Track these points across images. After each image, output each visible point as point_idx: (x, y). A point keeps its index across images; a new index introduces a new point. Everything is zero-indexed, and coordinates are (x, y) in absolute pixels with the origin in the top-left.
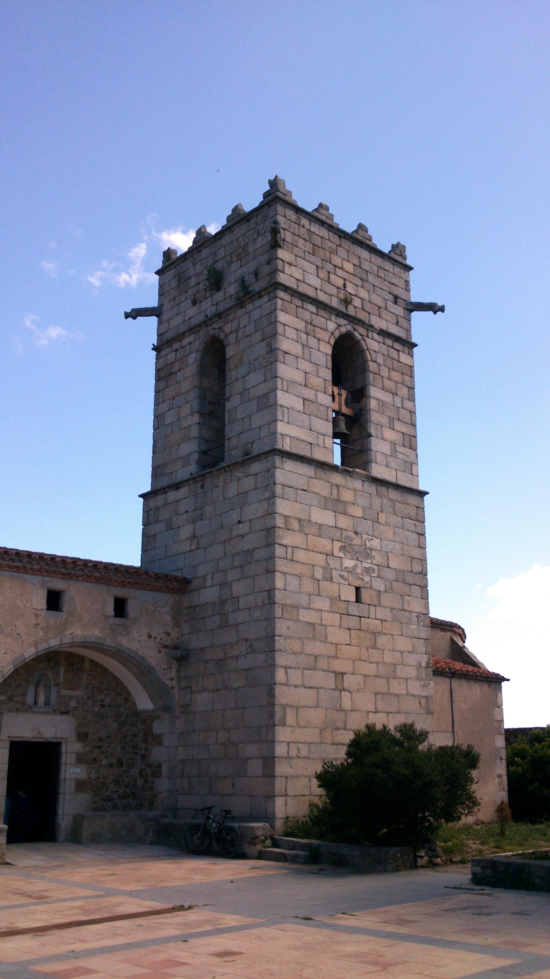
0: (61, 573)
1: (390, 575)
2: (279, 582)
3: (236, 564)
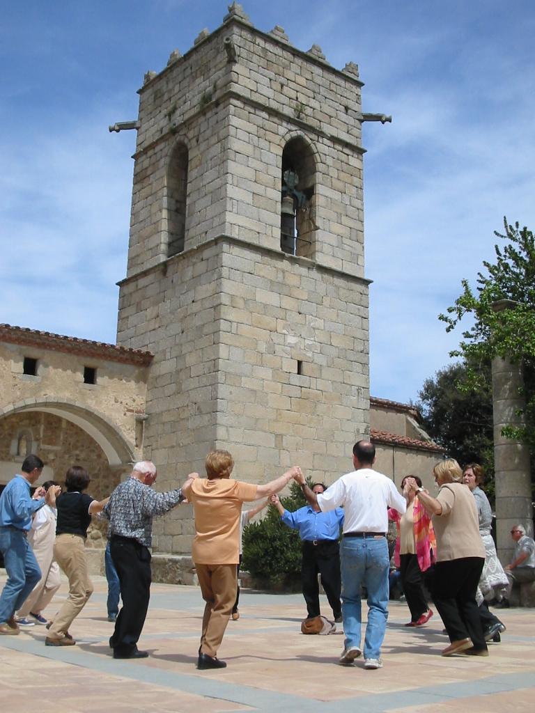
0: (37, 344)
1: (334, 352)
2: (223, 351)
3: (189, 338)
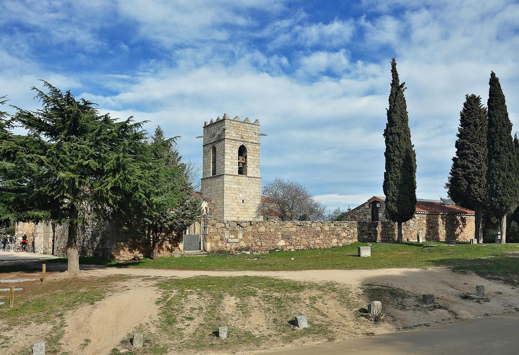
1: (251, 196)
